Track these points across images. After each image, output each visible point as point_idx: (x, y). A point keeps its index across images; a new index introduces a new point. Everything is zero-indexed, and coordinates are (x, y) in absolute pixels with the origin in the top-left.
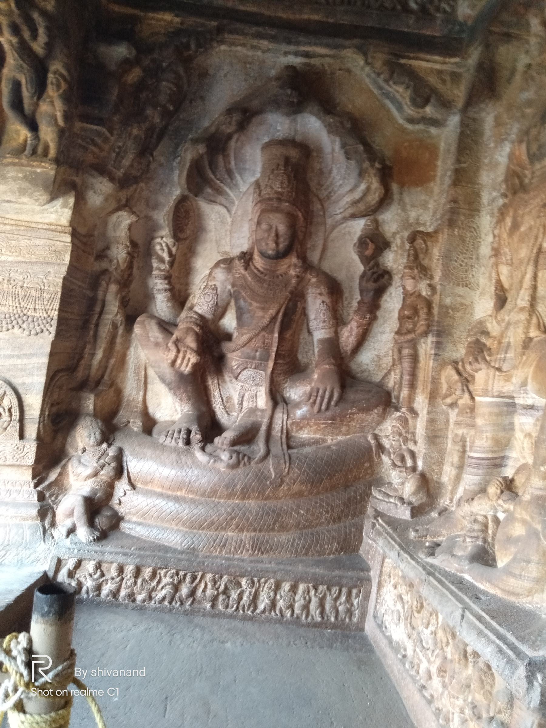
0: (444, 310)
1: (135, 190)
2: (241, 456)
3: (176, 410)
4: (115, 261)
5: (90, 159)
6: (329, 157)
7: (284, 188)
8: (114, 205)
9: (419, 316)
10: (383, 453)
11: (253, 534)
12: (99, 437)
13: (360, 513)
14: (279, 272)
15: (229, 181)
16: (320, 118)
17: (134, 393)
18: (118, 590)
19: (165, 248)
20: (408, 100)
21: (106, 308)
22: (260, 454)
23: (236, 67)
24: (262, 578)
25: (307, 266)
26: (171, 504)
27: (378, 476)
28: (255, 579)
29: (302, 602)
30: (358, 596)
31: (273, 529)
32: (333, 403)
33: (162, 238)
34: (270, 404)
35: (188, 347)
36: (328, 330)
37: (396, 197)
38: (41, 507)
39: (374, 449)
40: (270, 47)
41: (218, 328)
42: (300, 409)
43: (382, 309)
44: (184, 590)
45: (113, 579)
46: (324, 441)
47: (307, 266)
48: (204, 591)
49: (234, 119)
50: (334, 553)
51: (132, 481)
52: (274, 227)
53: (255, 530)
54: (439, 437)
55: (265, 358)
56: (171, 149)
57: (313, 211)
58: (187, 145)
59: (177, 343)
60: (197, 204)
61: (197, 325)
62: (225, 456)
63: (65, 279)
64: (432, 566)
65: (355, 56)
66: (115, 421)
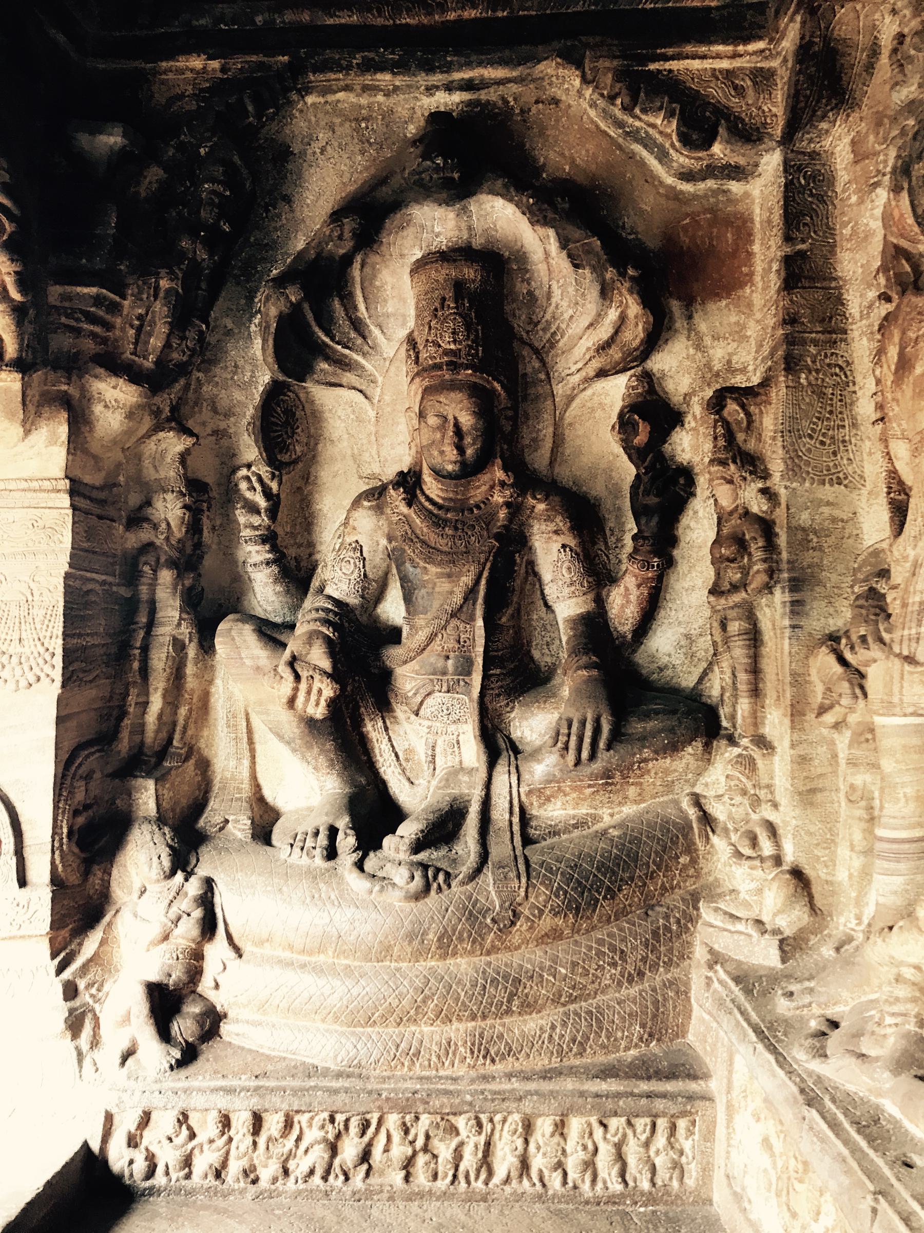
0: (799, 537)
1: (187, 387)
2: (430, 873)
5: (89, 346)
6: (540, 269)
7: (460, 343)
8: (148, 422)
9: (750, 555)
10: (713, 831)
11: (471, 1025)
12: (167, 863)
13: (682, 957)
15: (359, 341)
17: (232, 763)
18: (224, 1164)
19: (257, 486)
21: (160, 614)
22: (468, 864)
23: (344, 130)
24: (495, 1112)
25: (526, 480)
27: (711, 879)
28: (484, 1118)
30: (690, 1133)
31: (509, 1012)
32: (602, 745)
33: (249, 466)
34: (483, 758)
35: (315, 668)
37: (680, 323)
38: (71, 1011)
39: (695, 825)
40: (397, 83)
42: (539, 762)
43: (682, 544)
44: (350, 1150)
45: (211, 1141)
46: (596, 818)
47: (526, 480)
48: (386, 1150)
49: (347, 229)
50: (636, 1046)
51: (236, 940)
52: (450, 417)
53: (473, 1017)
54: (821, 790)
55: (465, 668)
56: (243, 302)
60: (307, 393)
62: (400, 876)
63: (67, 576)
64: (819, 1080)
65: (560, 71)
66: (201, 823)
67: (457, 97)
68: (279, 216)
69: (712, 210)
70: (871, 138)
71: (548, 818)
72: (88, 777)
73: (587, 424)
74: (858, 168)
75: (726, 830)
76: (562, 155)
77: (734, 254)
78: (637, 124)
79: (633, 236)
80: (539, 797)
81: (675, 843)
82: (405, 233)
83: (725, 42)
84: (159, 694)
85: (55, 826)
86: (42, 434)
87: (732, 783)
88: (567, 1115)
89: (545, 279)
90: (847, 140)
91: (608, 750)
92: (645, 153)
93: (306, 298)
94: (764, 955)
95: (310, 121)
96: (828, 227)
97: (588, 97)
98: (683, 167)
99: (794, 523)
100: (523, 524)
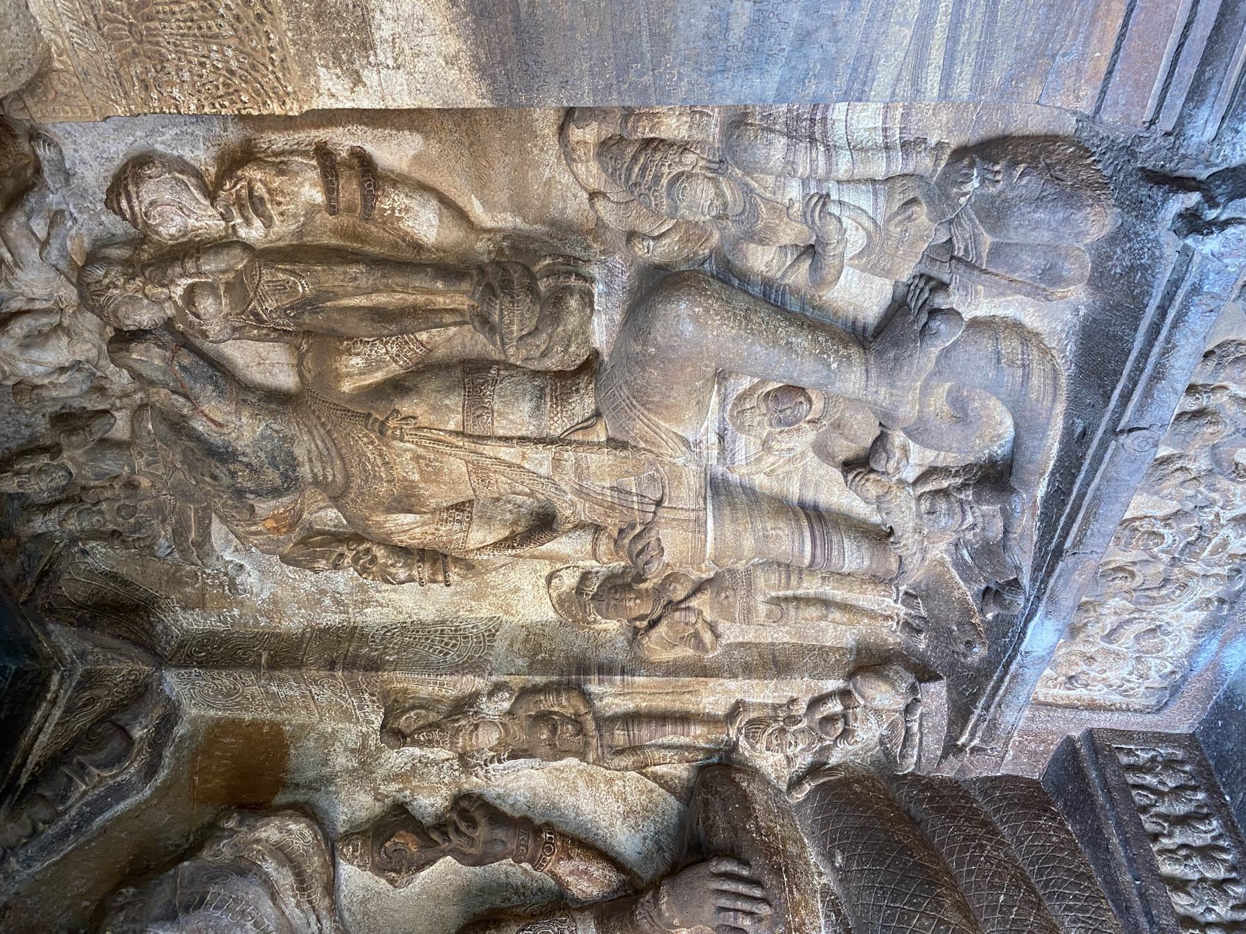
10: (826, 764)
20: (106, 774)
29: (1196, 861)
32: (745, 873)
37: (300, 797)
43: (529, 814)
46: (826, 891)
50: (1061, 822)
54: (774, 656)
64: (1036, 568)
69: (196, 753)
70: (188, 590)
75: (823, 749)
78: (73, 812)
79: (191, 839)
81: (841, 796)
83: (36, 708)
87: (775, 742)
88: (1160, 875)
90: (180, 614)
91: (750, 866)
92: (107, 815)
94: (936, 695)
98: (139, 771)
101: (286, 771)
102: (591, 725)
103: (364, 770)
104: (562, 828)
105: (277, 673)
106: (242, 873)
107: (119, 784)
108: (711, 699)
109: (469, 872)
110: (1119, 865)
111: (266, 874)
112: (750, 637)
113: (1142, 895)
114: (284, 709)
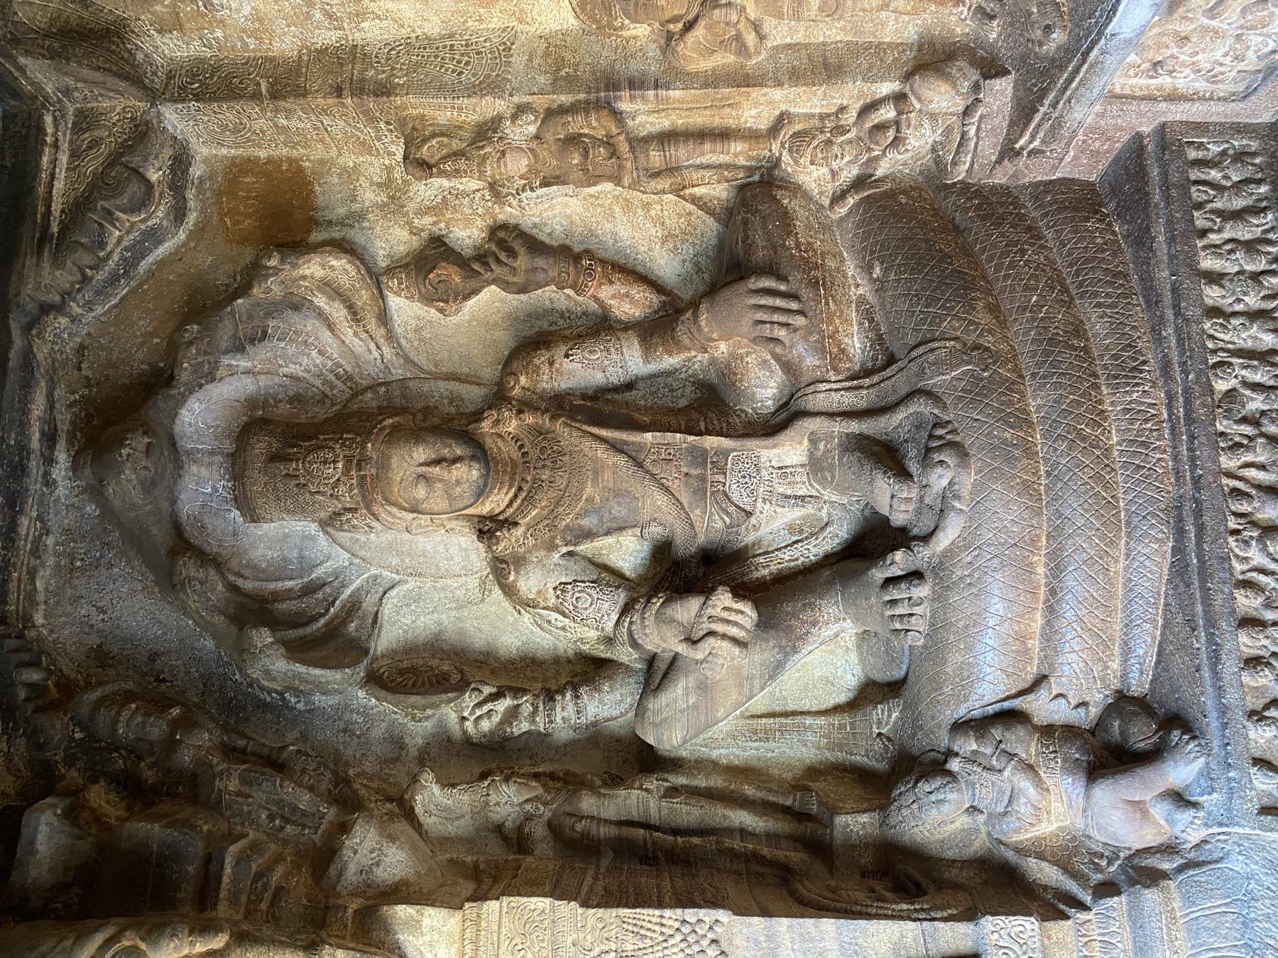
3: (837, 635)
4: (528, 807)
5: (300, 884)
6: (263, 381)
8: (403, 826)
9: (580, 135)
10: (872, 176)
11: (1105, 390)
12: (938, 782)
13: (1009, 194)
14: (516, 455)
15: (328, 590)
16: (182, 401)
17: (810, 737)
19: (486, 708)
21: (635, 815)
24: (1205, 347)
26: (1070, 582)
30: (1201, 146)
31: (1086, 350)
32: (783, 288)
33: (464, 719)
35: (699, 615)
36: (625, 344)
37: (336, 233)
41: (642, 579)
43: (568, 242)
46: (861, 300)
48: (1262, 467)
50: (1110, 224)
51: (1026, 685)
52: (420, 470)
53: (1096, 387)
54: (825, 58)
55: (700, 457)
56: (269, 717)
57: (379, 408)
58: (255, 673)
59: (693, 642)
60: (383, 656)
61: (648, 601)
62: (939, 479)
63: (586, 904)
66: (882, 766)
67: (62, 456)
68: (172, 668)
69: (219, 194)
70: (158, 8)
71: (863, 353)
72: (834, 891)
73: (437, 347)
74: (187, 26)
75: (870, 160)
76: (142, 344)
77: (267, 175)
78: (116, 257)
80: (840, 360)
81: (885, 208)
82: (210, 526)
84: (730, 813)
85: (901, 918)
86: (407, 940)
87: (820, 155)
88: (1198, 270)
89: (276, 379)
92: (150, 259)
93: (273, 631)
94: (1001, 91)
95: (65, 623)
96: (246, 63)
97: (80, 311)
99: (549, 88)
100: (541, 398)
101: (315, 209)
102: (624, 147)
103: (395, 203)
104: (602, 254)
105: (282, 103)
106: (296, 308)
107: (152, 229)
108: (753, 112)
109: (515, 300)
110: (1160, 262)
111: (319, 308)
112: (799, 37)
113: (1174, 290)
114: (298, 143)
